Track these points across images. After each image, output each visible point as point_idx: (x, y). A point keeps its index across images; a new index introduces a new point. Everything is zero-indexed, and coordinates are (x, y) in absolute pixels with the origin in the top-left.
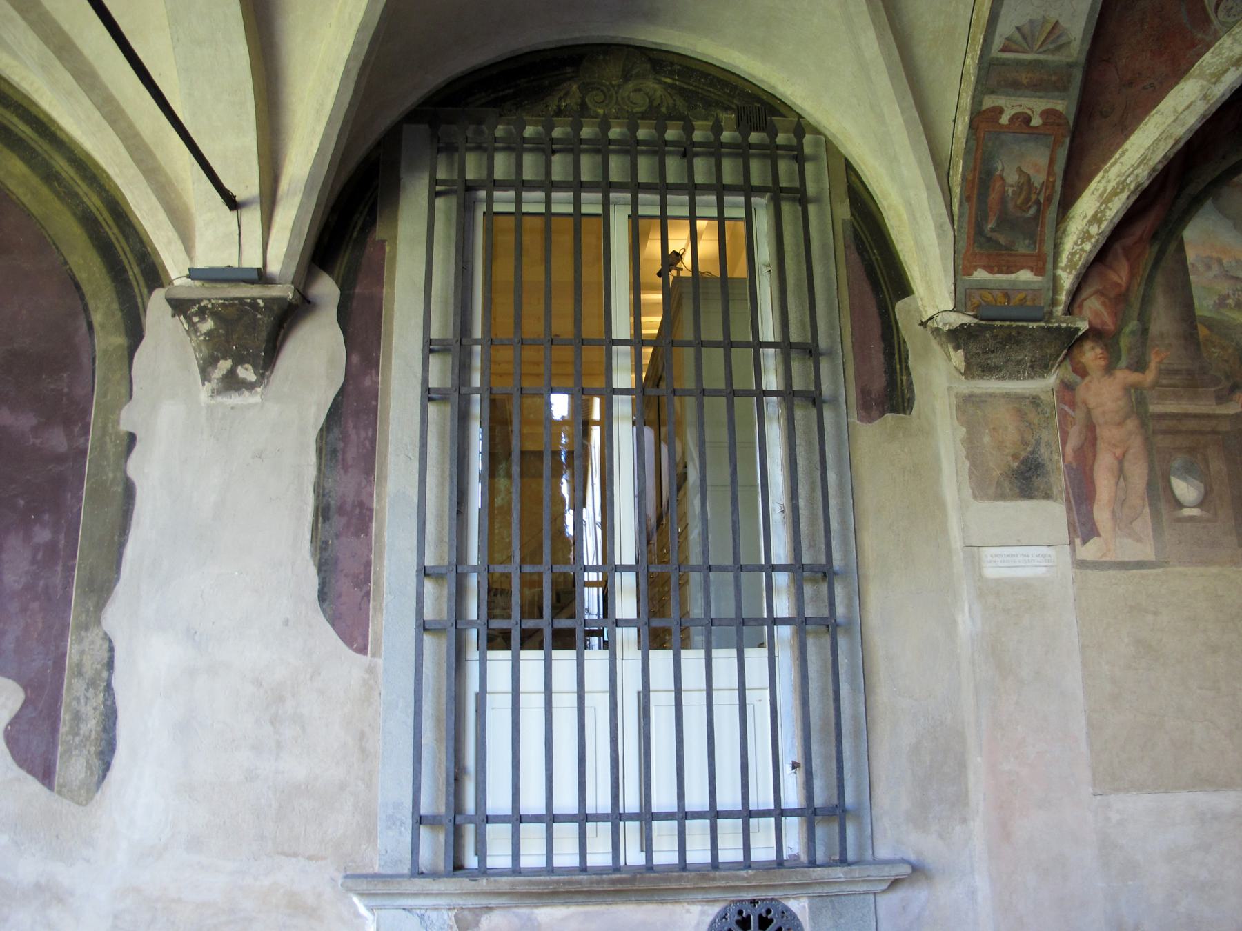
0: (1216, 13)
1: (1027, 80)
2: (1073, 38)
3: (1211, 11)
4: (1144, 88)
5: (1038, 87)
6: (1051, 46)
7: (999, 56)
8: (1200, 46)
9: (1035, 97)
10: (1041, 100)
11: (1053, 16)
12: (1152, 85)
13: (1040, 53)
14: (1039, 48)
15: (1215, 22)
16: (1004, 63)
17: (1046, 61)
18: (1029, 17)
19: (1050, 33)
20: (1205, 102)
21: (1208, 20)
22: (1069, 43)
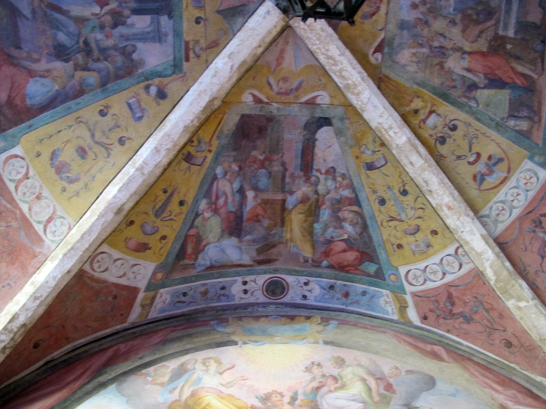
3: (41, 233)
8: (40, 256)
12: (9, 284)
15: (47, 241)
20: (33, 286)
21: (41, 240)
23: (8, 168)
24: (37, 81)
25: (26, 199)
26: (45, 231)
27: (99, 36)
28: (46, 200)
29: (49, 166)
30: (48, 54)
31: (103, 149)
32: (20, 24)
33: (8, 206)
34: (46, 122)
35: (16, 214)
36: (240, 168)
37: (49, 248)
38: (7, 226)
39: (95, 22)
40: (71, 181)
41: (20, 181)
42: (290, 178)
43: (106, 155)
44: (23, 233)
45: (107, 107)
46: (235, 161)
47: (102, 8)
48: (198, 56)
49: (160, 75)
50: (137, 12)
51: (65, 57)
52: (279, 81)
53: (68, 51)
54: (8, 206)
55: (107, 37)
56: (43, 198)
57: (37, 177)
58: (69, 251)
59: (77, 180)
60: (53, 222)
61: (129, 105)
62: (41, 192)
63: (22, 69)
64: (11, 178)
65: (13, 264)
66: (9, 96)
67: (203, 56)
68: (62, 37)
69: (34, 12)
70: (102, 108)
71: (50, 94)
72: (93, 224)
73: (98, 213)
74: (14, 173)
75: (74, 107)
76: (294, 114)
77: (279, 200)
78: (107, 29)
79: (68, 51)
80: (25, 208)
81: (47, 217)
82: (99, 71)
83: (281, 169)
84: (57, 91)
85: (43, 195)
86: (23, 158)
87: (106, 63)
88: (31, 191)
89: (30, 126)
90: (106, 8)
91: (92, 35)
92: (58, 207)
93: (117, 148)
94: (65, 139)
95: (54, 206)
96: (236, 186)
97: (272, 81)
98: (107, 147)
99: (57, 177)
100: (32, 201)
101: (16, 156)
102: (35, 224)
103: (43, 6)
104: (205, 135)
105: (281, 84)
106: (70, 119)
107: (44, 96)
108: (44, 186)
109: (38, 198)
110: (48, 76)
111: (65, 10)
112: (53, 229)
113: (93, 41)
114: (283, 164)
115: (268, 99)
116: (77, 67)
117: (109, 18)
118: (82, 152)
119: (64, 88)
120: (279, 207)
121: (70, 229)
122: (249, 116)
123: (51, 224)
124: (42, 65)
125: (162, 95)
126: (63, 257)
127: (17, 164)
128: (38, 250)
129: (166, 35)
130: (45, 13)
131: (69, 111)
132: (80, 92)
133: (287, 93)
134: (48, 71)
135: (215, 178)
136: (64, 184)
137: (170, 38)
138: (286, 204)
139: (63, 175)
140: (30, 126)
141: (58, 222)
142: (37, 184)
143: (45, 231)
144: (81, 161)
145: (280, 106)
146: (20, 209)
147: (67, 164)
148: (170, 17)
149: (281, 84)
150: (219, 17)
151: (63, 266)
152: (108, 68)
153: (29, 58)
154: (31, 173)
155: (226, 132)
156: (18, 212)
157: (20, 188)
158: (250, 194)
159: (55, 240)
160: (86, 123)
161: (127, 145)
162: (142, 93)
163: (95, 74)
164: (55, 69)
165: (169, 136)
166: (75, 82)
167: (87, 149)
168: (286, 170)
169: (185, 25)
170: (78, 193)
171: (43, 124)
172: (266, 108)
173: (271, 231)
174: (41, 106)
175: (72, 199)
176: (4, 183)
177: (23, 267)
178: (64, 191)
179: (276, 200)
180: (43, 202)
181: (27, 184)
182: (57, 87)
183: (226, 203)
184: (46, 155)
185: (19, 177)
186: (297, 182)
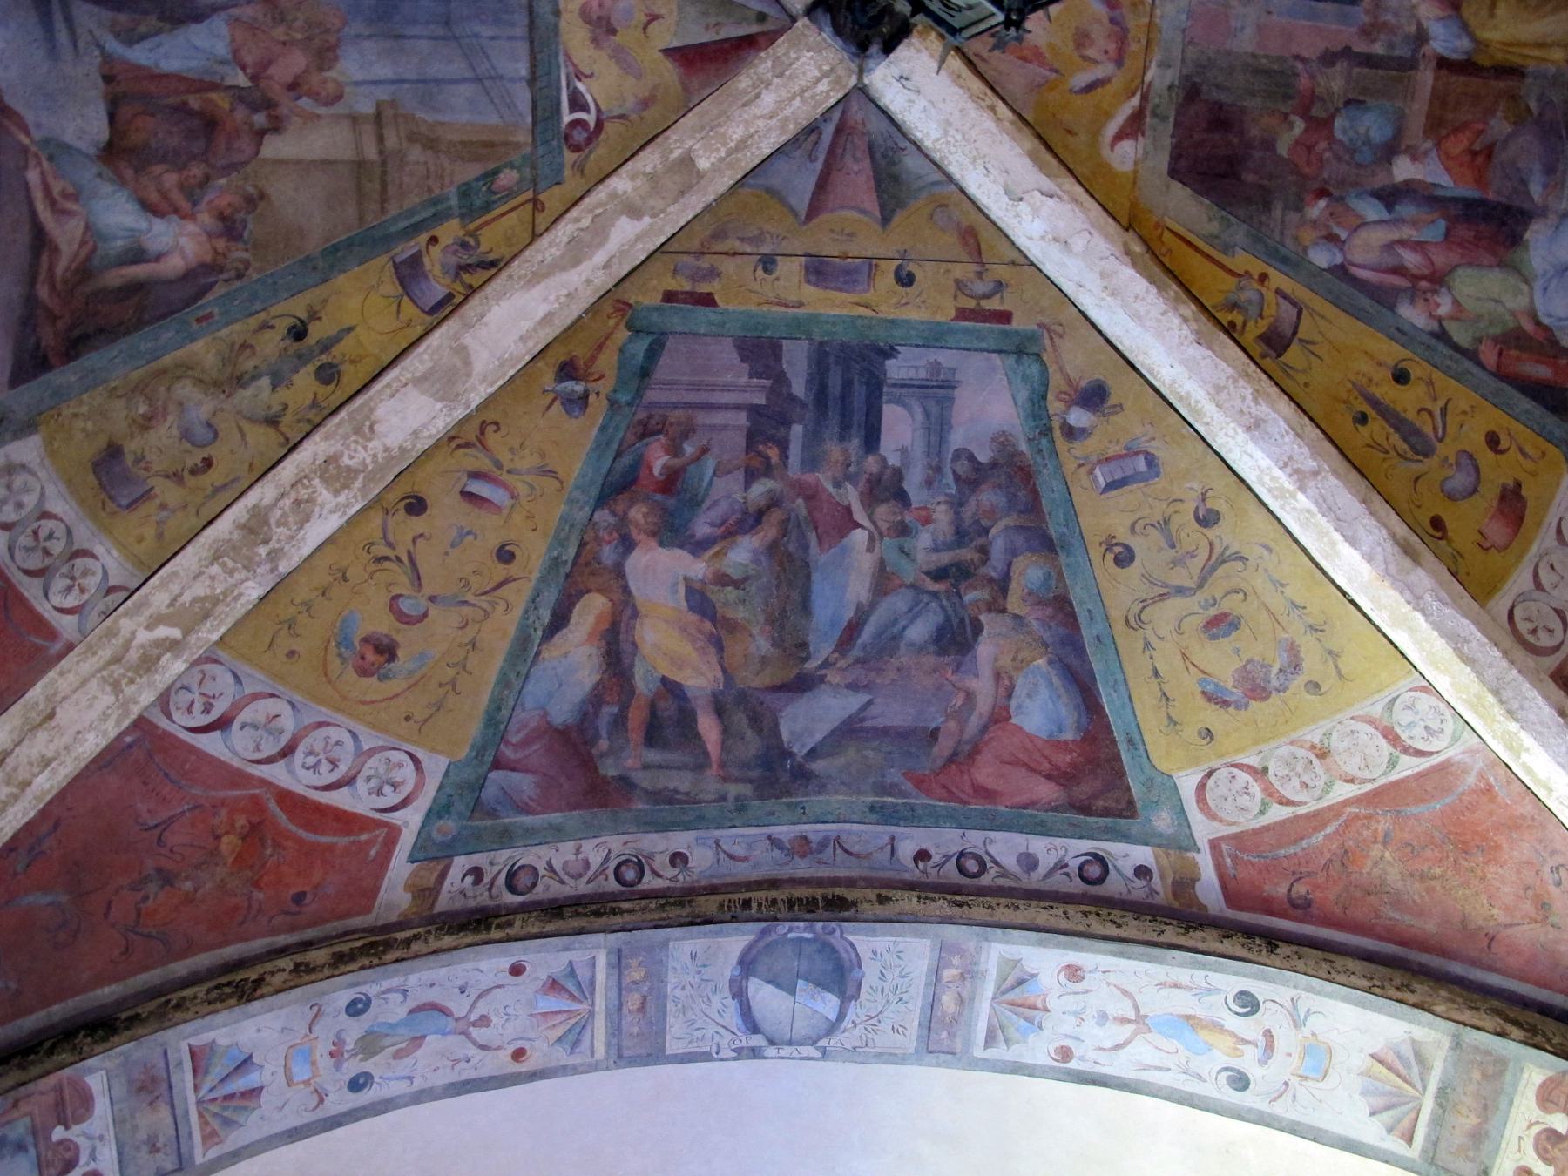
0: (1431, 753)
1: (1473, 1116)
2: (1406, 1036)
3: (1424, 764)
4: (1559, 884)
5: (1491, 1106)
6: (1415, 1069)
7: (1419, 1148)
8: (1492, 779)
9: (1508, 1112)
10: (1515, 1103)
11: (1360, 1061)
12: (1553, 870)
13: (1425, 1088)
14: (1414, 1087)
15: (1450, 753)
16: (1433, 1144)
17: (1441, 1081)
18: (1357, 1096)
19: (1390, 1068)
21: (1443, 768)
22: (1413, 1042)
23: (1228, 810)
24: (1019, 707)
25: (1321, 783)
26: (1420, 753)
27: (924, 539)
28: (1335, 735)
29: (1243, 712)
30: (956, 670)
31: (1220, 571)
32: (880, 723)
33: (1329, 830)
34: (1127, 700)
35: (1357, 817)
36: (1322, 193)
37: (1471, 752)
38: (1385, 843)
39: (888, 545)
40: (1295, 666)
41: (1269, 791)
42: (1374, 41)
43: (1239, 565)
44: (1413, 810)
45: (1110, 544)
46: (1299, 208)
47: (857, 525)
48: (1000, 286)
49: (1039, 399)
50: (871, 440)
51: (968, 629)
52: (1085, 58)
53: (955, 621)
54: (1329, 830)
55: (927, 521)
56: (1326, 742)
57: (1265, 747)
58: (1501, 702)
59: (1293, 650)
60: (1398, 729)
61: (1111, 486)
62: (1308, 745)
63: (986, 737)
64: (1256, 811)
65: (1498, 847)
66: (1049, 777)
67: (1002, 272)
68: (919, 631)
69: (854, 687)
70: (1110, 557)
71: (1056, 680)
72: (1436, 626)
73: (1407, 608)
74: (1243, 801)
75: (1098, 628)
76: (1183, 17)
77: (1436, 79)
78: (908, 518)
79: (955, 621)
80: (1343, 792)
81: (1383, 742)
82: (1013, 552)
83: (1343, 66)
84: (1050, 662)
85: (1316, 741)
86: (1210, 774)
87: (993, 531)
88: (1299, 769)
89: (1130, 741)
90: (859, 515)
91: (921, 557)
92: (1358, 711)
93: (1223, 534)
94: (1178, 662)
95: (1352, 718)
96: (1372, 210)
97: (1081, 79)
98: (1218, 560)
99: (1275, 699)
100: (1328, 771)
101: (1201, 787)
102: (1394, 776)
103: (842, 663)
104: (1217, 286)
105: (1091, 52)
106: (1128, 643)
107: (1059, 696)
108: (1294, 736)
109: (1323, 754)
110: (1010, 678)
111: (856, 613)
112: (1419, 731)
113: (934, 557)
114: (1329, 59)
115: (1133, 94)
116: (997, 606)
117: (882, 511)
118: (1220, 625)
119: (1045, 645)
120: (1458, 81)
121: (1429, 689)
122: (1176, 156)
123: (1404, 736)
124: (983, 688)
125: (1094, 397)
126: (1516, 720)
127: (1223, 790)
128: (1471, 780)
129: (936, 367)
130: (861, 661)
131: (1108, 641)
132: (1062, 608)
133: (1121, 35)
134: (998, 676)
135: (1341, 271)
136: (1299, 681)
137: (946, 358)
138: (1455, 56)
139: (1275, 683)
140: (1130, 741)
141: (1401, 717)
142: (1285, 750)
143: (1420, 753)
144: (1244, 632)
145: (1157, 56)
146: (1346, 803)
147: (1245, 666)
148: (889, 352)
149: (1091, 52)
150: (896, 219)
151: (1542, 723)
152: (1007, 528)
153: (961, 715)
154: (1253, 760)
155: (1214, 227)
156: (1352, 810)
157: (1288, 793)
158: (1403, 170)
159: (1454, 732)
160: (1145, 603)
161: (1219, 505)
162: (1080, 448)
163: (1019, 563)
164: (996, 660)
165: (1219, 389)
166: (1034, 618)
167: (1213, 612)
168: (1346, 52)
169: (913, 315)
170: (1330, 652)
171: (1129, 710)
172: (1157, 101)
173: (1529, 110)
174: (1082, 707)
175: (1343, 672)
176: (1267, 828)
177: (1515, 825)
178: (1317, 686)
179: (1434, 88)
180: (1336, 743)
181: (1279, 774)
182: (1041, 662)
183: (1418, 246)
184: (1212, 716)
185: (1256, 789)
186: (1389, 17)
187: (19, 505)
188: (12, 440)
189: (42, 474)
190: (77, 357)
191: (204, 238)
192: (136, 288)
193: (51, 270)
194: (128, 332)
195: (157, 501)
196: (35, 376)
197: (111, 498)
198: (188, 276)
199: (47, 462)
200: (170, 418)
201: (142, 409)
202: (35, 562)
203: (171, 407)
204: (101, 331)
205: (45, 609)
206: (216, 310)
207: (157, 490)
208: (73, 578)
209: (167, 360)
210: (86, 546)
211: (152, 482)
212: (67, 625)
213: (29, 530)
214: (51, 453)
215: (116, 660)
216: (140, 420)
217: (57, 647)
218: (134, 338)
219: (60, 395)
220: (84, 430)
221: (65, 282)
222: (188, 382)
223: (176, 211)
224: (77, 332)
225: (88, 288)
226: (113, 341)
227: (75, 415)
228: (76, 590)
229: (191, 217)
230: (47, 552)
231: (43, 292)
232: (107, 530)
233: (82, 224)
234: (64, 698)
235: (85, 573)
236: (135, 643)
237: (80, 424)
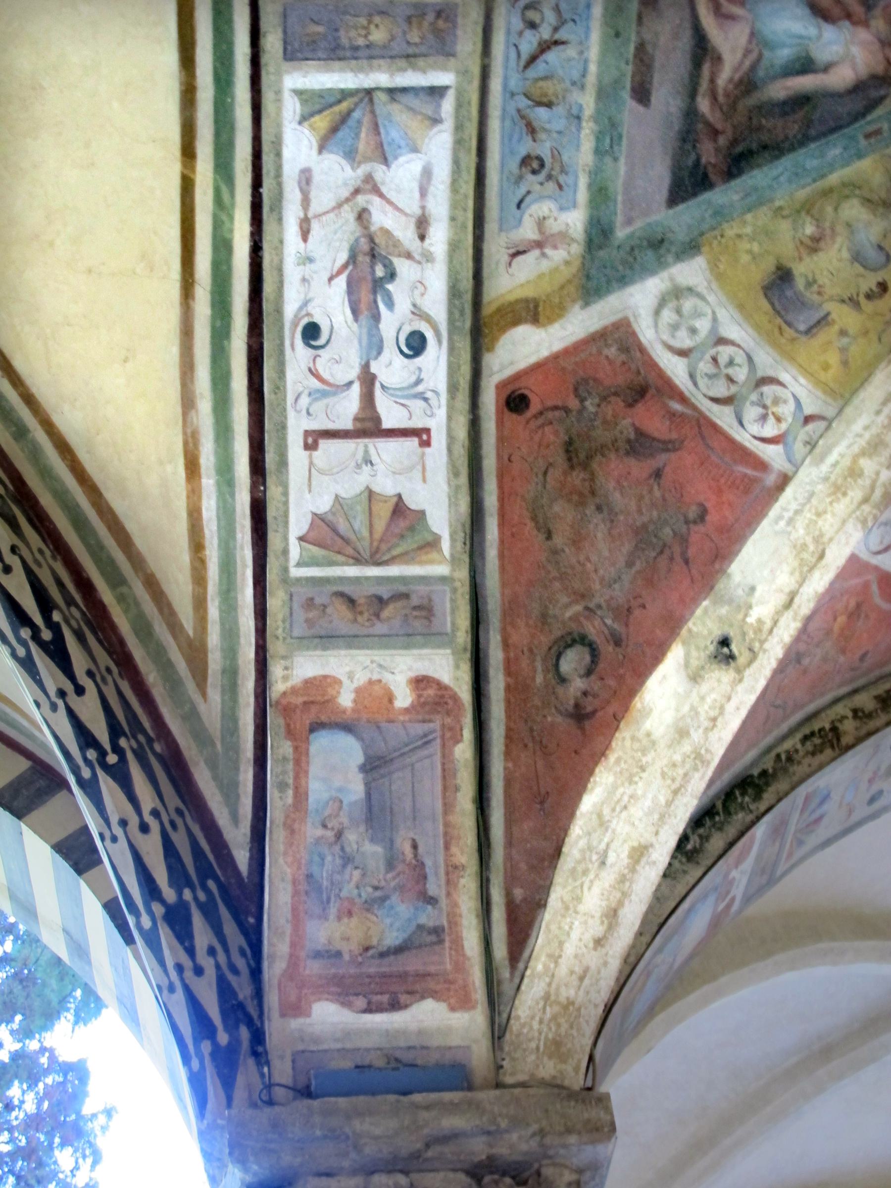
187: (693, 331)
188: (675, 263)
189: (711, 298)
190: (740, 173)
191: (877, 46)
192: (802, 100)
193: (712, 81)
194: (792, 149)
195: (836, 328)
196: (695, 195)
197: (789, 324)
198: (858, 88)
199: (714, 286)
200: (839, 240)
201: (809, 229)
202: (721, 389)
203: (839, 228)
204: (765, 147)
205: (743, 437)
206: (885, 126)
207: (834, 316)
208: (765, 407)
209: (834, 178)
210: (771, 373)
211: (829, 306)
212: (772, 454)
213: (708, 357)
214: (718, 276)
215: (866, 500)
216: (809, 243)
217: (770, 480)
218: (800, 155)
219: (721, 214)
220: (750, 252)
221: (727, 95)
222: (855, 202)
223: (849, 16)
224: (739, 149)
225: (751, 101)
226: (777, 158)
227: (739, 236)
228: (771, 420)
229: (865, 24)
230: (730, 380)
231: (704, 105)
232: (792, 359)
233: (747, 31)
234: (831, 540)
235: (776, 401)
236: (879, 483)
237: (745, 245)
